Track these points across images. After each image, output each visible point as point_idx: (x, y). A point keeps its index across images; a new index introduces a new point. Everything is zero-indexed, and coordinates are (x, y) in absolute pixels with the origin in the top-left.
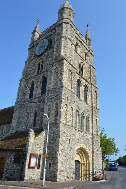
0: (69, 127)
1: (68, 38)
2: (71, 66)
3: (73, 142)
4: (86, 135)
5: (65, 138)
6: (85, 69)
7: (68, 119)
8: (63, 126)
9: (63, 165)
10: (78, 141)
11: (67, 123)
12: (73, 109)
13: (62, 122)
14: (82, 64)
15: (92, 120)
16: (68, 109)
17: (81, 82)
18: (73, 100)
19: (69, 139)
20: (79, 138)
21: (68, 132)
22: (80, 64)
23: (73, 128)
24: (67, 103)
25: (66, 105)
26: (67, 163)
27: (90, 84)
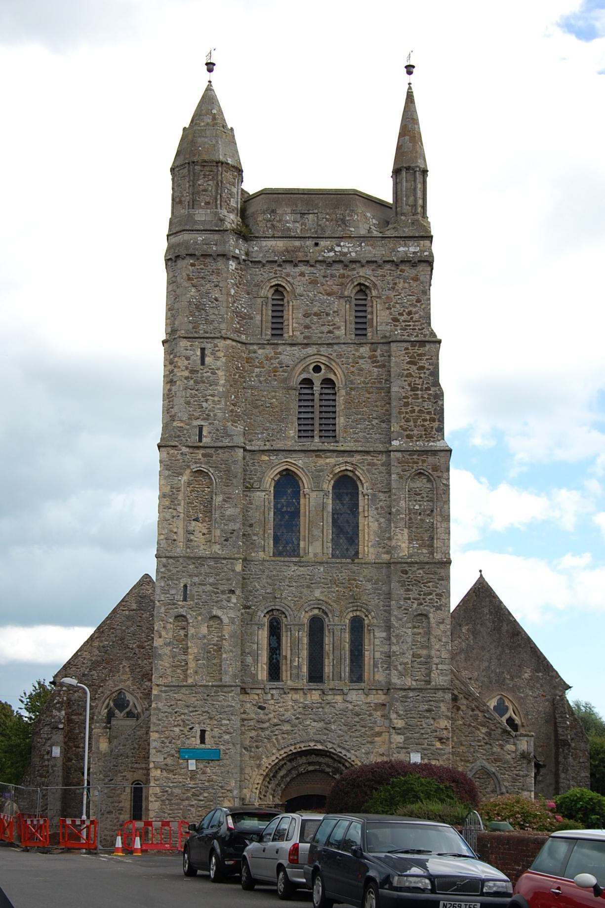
0: (201, 689)
1: (180, 337)
2: (202, 451)
3: (227, 737)
4: (339, 698)
5: (177, 729)
6: (343, 392)
7: (192, 665)
8: (164, 695)
9: (171, 810)
10: (286, 727)
11: (190, 681)
12: (226, 620)
13: (161, 681)
14: (317, 379)
15: (388, 628)
16: (191, 631)
17: (301, 479)
18: (226, 588)
19: (197, 729)
20: (288, 715)
21: (191, 709)
22: (308, 382)
23: (226, 689)
24: (182, 611)
25: (179, 617)
26: (194, 802)
27: (381, 452)
